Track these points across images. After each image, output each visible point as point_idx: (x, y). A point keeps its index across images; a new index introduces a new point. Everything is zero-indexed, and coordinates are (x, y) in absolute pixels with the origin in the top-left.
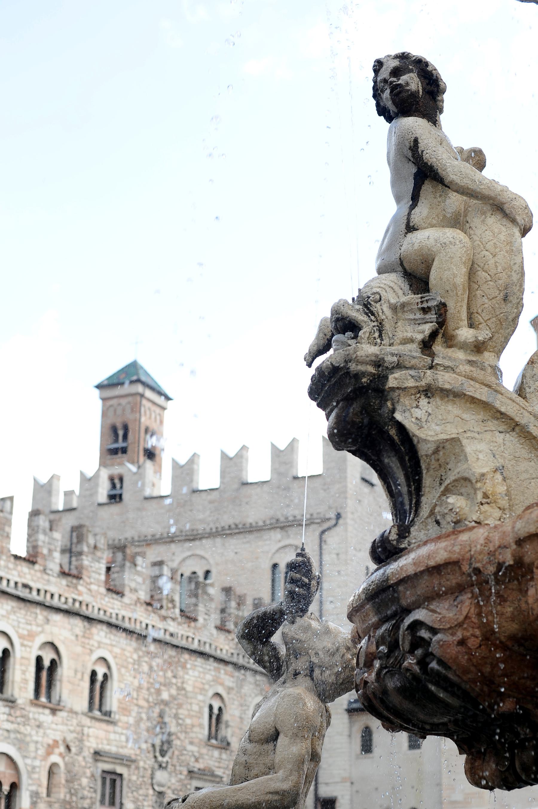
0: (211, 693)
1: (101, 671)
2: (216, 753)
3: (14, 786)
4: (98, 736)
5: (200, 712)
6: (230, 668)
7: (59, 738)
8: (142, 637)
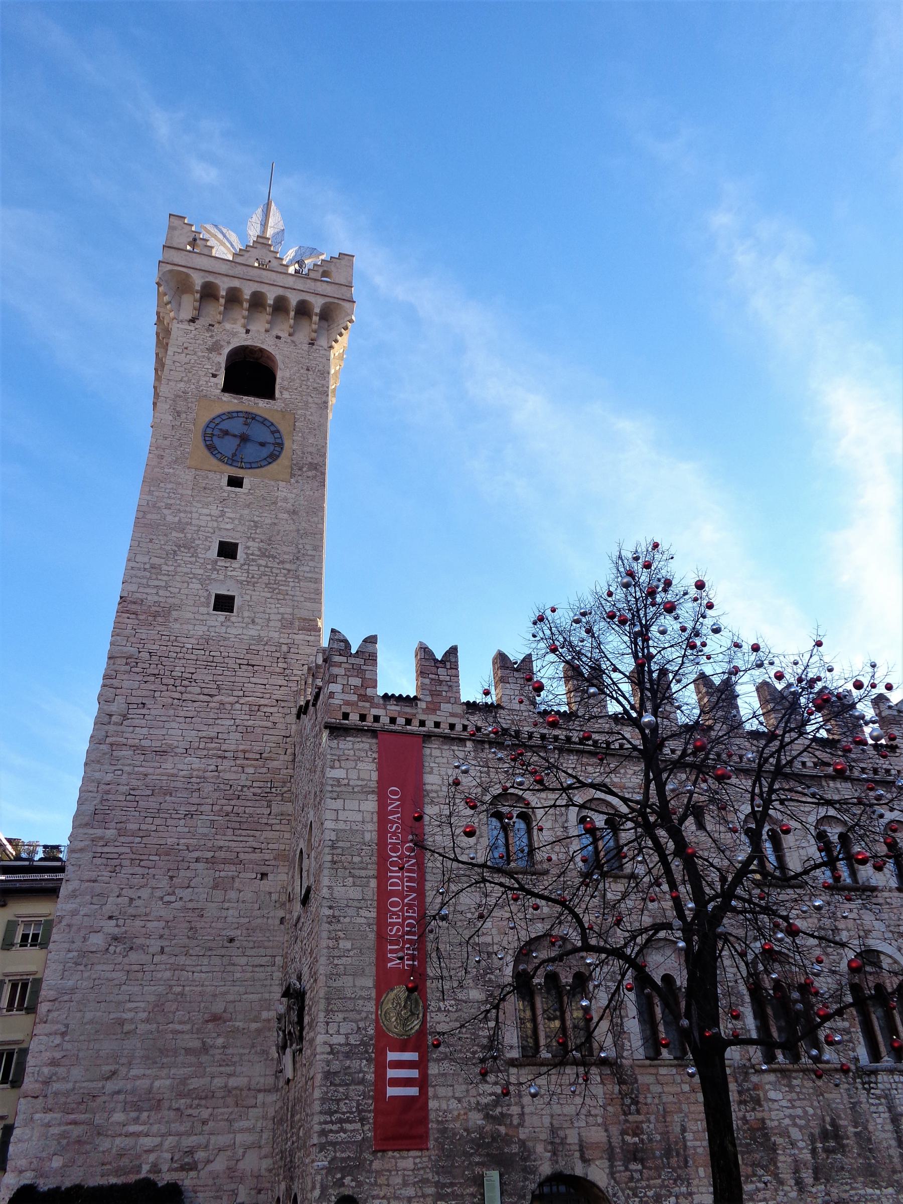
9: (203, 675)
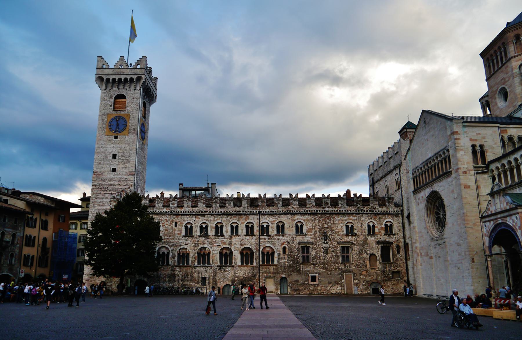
0: (346, 222)
1: (299, 225)
2: (350, 237)
3: (273, 253)
4: (299, 239)
5: (342, 228)
6: (354, 215)
7: (285, 241)
8: (315, 214)
9: (110, 188)
